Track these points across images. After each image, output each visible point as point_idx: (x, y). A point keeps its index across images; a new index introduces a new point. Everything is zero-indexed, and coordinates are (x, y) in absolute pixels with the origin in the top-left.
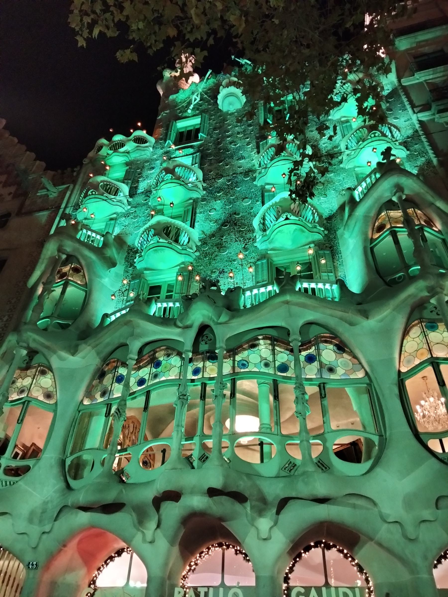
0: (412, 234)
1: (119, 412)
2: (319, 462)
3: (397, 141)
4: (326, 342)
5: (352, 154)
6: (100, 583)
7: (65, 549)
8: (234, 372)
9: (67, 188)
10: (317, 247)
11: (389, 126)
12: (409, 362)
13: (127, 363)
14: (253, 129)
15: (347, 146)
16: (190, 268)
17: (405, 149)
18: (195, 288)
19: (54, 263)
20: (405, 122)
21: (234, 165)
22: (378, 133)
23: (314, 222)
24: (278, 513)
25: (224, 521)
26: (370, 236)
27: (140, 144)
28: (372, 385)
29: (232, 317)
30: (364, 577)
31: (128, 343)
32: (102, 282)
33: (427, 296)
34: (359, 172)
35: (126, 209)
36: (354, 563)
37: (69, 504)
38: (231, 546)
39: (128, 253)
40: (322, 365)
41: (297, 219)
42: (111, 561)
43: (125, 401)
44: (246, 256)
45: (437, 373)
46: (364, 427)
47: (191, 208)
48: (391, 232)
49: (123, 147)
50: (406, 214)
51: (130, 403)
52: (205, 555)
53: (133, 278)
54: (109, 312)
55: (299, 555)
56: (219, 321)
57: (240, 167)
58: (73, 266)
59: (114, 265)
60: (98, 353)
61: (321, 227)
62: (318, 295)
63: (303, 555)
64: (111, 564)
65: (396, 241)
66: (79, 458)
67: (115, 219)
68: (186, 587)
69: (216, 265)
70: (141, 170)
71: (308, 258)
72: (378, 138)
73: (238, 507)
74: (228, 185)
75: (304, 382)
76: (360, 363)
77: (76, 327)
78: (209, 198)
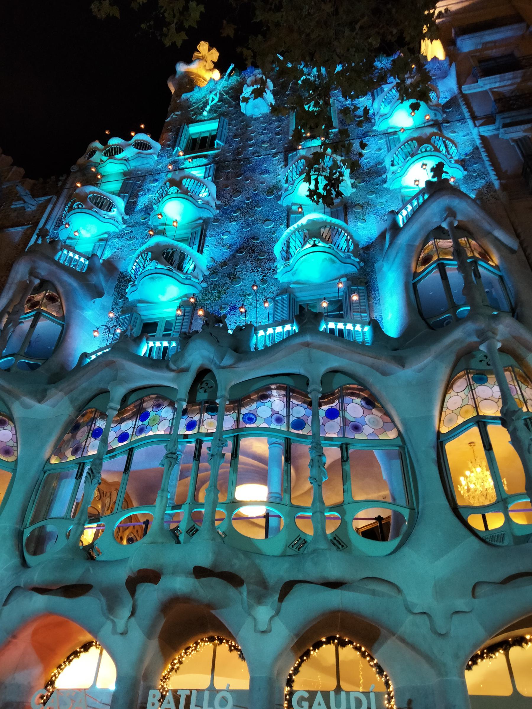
0: (462, 267)
1: (92, 472)
2: (335, 538)
3: (452, 158)
4: (353, 394)
5: (398, 171)
6: (59, 684)
7: (15, 641)
8: (238, 428)
10: (350, 282)
11: (444, 139)
12: (450, 420)
13: (107, 413)
14: (281, 138)
15: (393, 161)
16: (192, 300)
17: (462, 169)
19: (24, 288)
21: (255, 180)
23: (348, 251)
24: (281, 599)
25: (213, 609)
26: (413, 269)
29: (239, 360)
30: (383, 680)
31: (109, 389)
33: (476, 342)
34: (405, 194)
35: (120, 228)
36: (372, 663)
37: (22, 585)
38: (224, 641)
39: (120, 282)
40: (345, 421)
41: (327, 246)
42: (75, 657)
43: (101, 459)
45: (483, 433)
46: (394, 499)
47: (199, 229)
48: (438, 264)
49: (120, 153)
50: (456, 243)
51: (107, 464)
52: (192, 651)
53: (123, 312)
54: (89, 352)
55: (307, 653)
56: (221, 365)
57: (262, 183)
58: (47, 294)
59: (100, 294)
60: (72, 401)
63: (312, 652)
64: (75, 661)
66: (42, 528)
67: (106, 240)
68: (166, 689)
70: (142, 182)
71: (337, 295)
72: (429, 153)
73: (232, 591)
74: (247, 204)
75: (322, 442)
76: (393, 422)
77: (46, 367)
78: (223, 219)
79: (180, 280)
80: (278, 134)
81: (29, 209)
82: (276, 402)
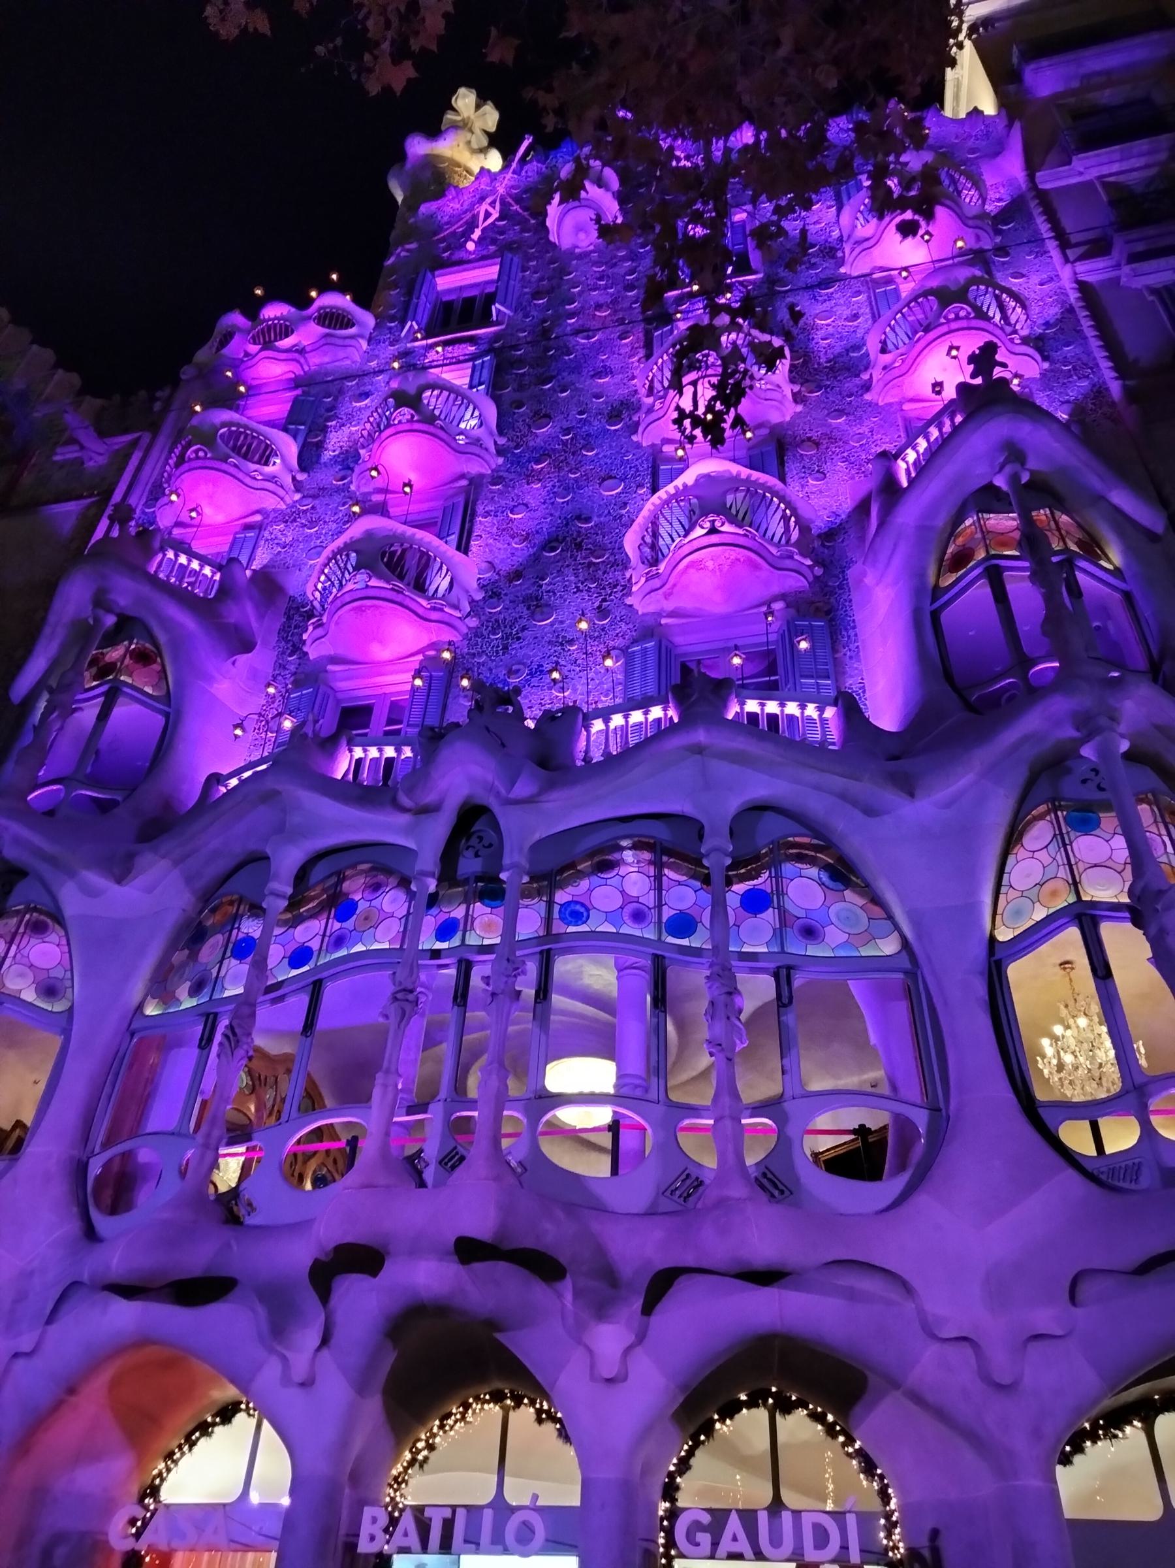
0: (1040, 575)
2: (764, 1175)
3: (1015, 332)
4: (800, 858)
5: (897, 364)
6: (168, 1494)
7: (73, 1399)
9: (135, 443)
10: (792, 611)
12: (1018, 914)
13: (264, 905)
15: (884, 343)
16: (446, 655)
17: (1038, 357)
18: (460, 709)
19: (83, 633)
20: (1041, 284)
22: (965, 310)
24: (648, 1309)
25: (500, 1330)
26: (932, 580)
27: (335, 328)
28: (919, 974)
29: (549, 786)
31: (269, 851)
32: (212, 691)
33: (1073, 740)
34: (912, 415)
35: (289, 501)
36: (851, 1450)
37: (85, 1278)
38: (526, 1401)
39: (289, 618)
41: (741, 532)
42: (202, 1435)
43: (253, 1006)
44: (603, 630)
45: (1090, 942)
46: (894, 1088)
47: (461, 499)
48: (986, 569)
49: (287, 336)
51: (264, 1013)
52: (456, 1422)
53: (298, 685)
54: (225, 772)
55: (708, 1429)
56: (511, 796)
57: (598, 397)
58: (133, 647)
59: (247, 646)
60: (189, 880)
61: (805, 556)
62: (784, 731)
63: (718, 1426)
65: (1000, 595)
66: (128, 1156)
67: (260, 527)
68: (401, 1506)
69: (521, 653)
70: (336, 399)
72: (964, 323)
73: (539, 1291)
74: (565, 443)
76: (890, 917)
77: (132, 807)
78: (512, 476)
79: (420, 611)
80: (630, 287)
81: (91, 464)
82: (633, 874)
